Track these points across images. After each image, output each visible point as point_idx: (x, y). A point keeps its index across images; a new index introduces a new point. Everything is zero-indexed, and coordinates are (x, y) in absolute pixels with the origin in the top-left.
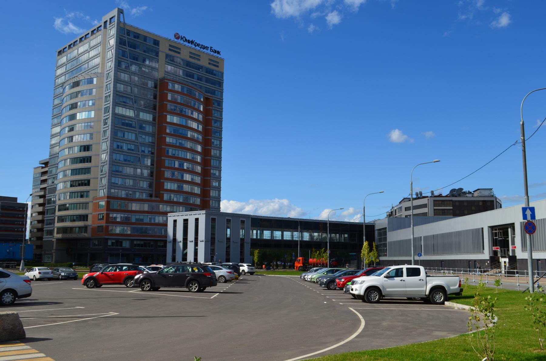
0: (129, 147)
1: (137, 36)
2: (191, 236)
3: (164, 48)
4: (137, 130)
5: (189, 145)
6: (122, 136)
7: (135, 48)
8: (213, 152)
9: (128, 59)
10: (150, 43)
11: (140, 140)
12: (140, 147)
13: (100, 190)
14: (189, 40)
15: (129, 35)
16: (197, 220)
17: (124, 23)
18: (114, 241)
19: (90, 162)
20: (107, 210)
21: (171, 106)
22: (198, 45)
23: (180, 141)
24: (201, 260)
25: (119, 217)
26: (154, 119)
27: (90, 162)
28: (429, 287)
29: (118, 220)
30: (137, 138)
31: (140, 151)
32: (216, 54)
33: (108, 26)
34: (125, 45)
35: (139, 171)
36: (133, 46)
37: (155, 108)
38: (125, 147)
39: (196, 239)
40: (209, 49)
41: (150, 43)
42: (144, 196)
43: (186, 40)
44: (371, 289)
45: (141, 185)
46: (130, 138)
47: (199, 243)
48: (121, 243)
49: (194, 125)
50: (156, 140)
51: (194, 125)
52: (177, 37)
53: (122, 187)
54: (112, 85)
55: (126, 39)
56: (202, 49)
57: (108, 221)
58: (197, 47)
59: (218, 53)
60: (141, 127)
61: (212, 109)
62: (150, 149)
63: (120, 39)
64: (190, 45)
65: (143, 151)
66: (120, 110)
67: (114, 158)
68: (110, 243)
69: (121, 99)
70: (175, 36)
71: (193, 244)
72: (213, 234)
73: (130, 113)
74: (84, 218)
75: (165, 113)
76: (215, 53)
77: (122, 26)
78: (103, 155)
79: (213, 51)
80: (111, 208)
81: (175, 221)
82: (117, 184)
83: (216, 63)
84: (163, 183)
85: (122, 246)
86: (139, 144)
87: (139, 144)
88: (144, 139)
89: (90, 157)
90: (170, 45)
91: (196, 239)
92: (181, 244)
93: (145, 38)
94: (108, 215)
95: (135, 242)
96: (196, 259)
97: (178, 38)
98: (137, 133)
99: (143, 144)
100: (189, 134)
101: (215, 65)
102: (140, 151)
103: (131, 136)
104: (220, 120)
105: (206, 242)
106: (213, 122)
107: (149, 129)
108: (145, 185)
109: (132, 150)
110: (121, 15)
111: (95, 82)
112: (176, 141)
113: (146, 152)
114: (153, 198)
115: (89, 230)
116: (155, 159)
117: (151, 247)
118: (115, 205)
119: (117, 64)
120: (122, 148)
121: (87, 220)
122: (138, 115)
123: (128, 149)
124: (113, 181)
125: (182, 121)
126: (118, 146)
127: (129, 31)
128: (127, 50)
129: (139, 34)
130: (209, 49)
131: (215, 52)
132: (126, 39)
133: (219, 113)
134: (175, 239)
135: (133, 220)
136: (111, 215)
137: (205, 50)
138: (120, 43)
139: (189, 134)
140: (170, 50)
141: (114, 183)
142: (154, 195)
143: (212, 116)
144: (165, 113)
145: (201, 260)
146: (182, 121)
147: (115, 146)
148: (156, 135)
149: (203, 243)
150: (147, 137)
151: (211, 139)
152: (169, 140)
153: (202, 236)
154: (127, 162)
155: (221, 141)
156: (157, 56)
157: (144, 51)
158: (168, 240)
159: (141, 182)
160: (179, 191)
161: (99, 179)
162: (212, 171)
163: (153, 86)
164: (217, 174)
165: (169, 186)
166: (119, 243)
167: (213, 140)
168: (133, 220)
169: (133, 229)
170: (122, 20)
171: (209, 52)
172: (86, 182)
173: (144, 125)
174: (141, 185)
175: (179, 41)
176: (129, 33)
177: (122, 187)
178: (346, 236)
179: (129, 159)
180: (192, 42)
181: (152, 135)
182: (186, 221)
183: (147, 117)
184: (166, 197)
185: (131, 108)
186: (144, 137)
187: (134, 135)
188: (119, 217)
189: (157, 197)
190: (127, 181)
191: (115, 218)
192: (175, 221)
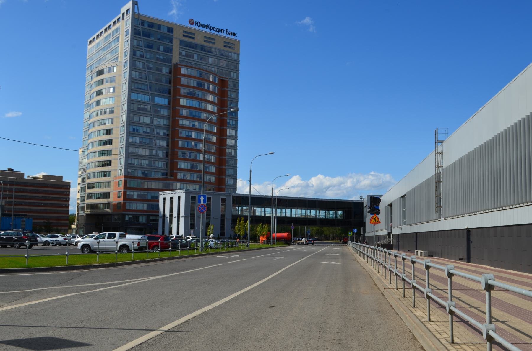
0: (145, 130)
1: (151, 25)
2: (175, 213)
3: (178, 35)
4: (152, 114)
5: (205, 126)
6: (138, 120)
7: (149, 37)
8: (229, 132)
9: (143, 48)
10: (164, 30)
11: (155, 122)
12: (155, 130)
13: (118, 170)
14: (204, 25)
15: (143, 25)
16: (179, 198)
17: (139, 14)
18: (131, 216)
19: (112, 144)
20: (124, 189)
21: (184, 90)
22: (213, 29)
23: (194, 123)
24: (182, 233)
25: (135, 194)
26: (169, 103)
27: (112, 144)
28: (119, 244)
29: (135, 197)
30: (152, 121)
31: (156, 133)
32: (233, 37)
33: (125, 17)
34: (139, 34)
35: (154, 152)
36: (148, 35)
37: (170, 93)
38: (141, 131)
39: (179, 215)
40: (225, 32)
41: (164, 30)
42: (160, 176)
43: (201, 25)
44: (86, 246)
45: (157, 165)
46: (145, 121)
47: (173, 218)
48: (138, 218)
49: (210, 107)
50: (171, 122)
51: (210, 107)
52: (192, 22)
53: (138, 167)
54: (127, 74)
55: (141, 29)
56: (217, 33)
57: (125, 199)
58: (212, 31)
59: (235, 35)
60: (156, 111)
61: (227, 91)
62: (165, 131)
63: (135, 29)
64: (205, 29)
65: (158, 133)
66: (135, 96)
67: (130, 140)
68: (127, 218)
69: (136, 86)
70: (190, 22)
71: (176, 219)
72: (193, 210)
73: (145, 98)
74: (106, 195)
75: (178, 97)
76: (231, 35)
77: (137, 17)
78: (119, 137)
79: (229, 34)
80: (128, 186)
81: (164, 199)
82: (133, 164)
83: (232, 45)
84: (177, 162)
85: (138, 221)
86: (154, 127)
87: (154, 127)
88: (160, 122)
89: (112, 140)
90: (184, 32)
91: (179, 215)
92: (168, 219)
93: (159, 27)
94: (125, 193)
95: (151, 218)
96: (178, 233)
97: (192, 24)
98: (152, 116)
99: (159, 127)
100: (204, 115)
101: (230, 47)
102: (156, 133)
103: (146, 120)
104: (235, 102)
105: (186, 218)
106: (229, 103)
107: (164, 112)
108: (160, 165)
109: (148, 133)
110: (136, 6)
111: (115, 70)
112: (190, 123)
113: (162, 134)
114: (169, 177)
115: (111, 207)
116: (170, 140)
117: (150, 223)
118: (133, 183)
119: (132, 53)
120: (137, 130)
121: (109, 198)
122: (153, 100)
123: (144, 132)
124: (129, 162)
125: (195, 104)
126: (134, 130)
127: (144, 21)
128: (142, 40)
129: (154, 23)
130: (225, 32)
131: (231, 34)
132: (141, 29)
133: (234, 94)
134: (164, 215)
135: (149, 198)
136: (128, 193)
137: (220, 33)
138: (135, 34)
139: (204, 115)
140: (184, 36)
141: (131, 164)
142: (169, 174)
143: (227, 97)
144: (178, 97)
145: (182, 233)
146: (195, 104)
147: (131, 130)
148: (171, 118)
149: (183, 218)
150: (162, 120)
151: (226, 120)
152: (184, 122)
153: (182, 213)
154: (141, 145)
155: (237, 121)
156: (172, 43)
157: (159, 39)
158: (159, 214)
159: (157, 163)
160: (192, 170)
161: (119, 160)
162: (227, 150)
163: (168, 71)
164: (233, 153)
165: (183, 165)
166: (136, 218)
167: (228, 121)
168: (149, 198)
169: (148, 206)
170: (136, 11)
171: (224, 35)
172: (108, 162)
173: (159, 109)
174: (157, 165)
175: (194, 27)
176: (143, 23)
177: (138, 167)
178: (340, 213)
179: (144, 141)
180: (207, 26)
181: (168, 118)
182: (172, 198)
183: (164, 101)
184: (180, 176)
185: (146, 93)
186: (159, 120)
187: (149, 119)
188: (135, 194)
189: (171, 176)
190: (143, 161)
191: (133, 195)
192: (164, 199)
